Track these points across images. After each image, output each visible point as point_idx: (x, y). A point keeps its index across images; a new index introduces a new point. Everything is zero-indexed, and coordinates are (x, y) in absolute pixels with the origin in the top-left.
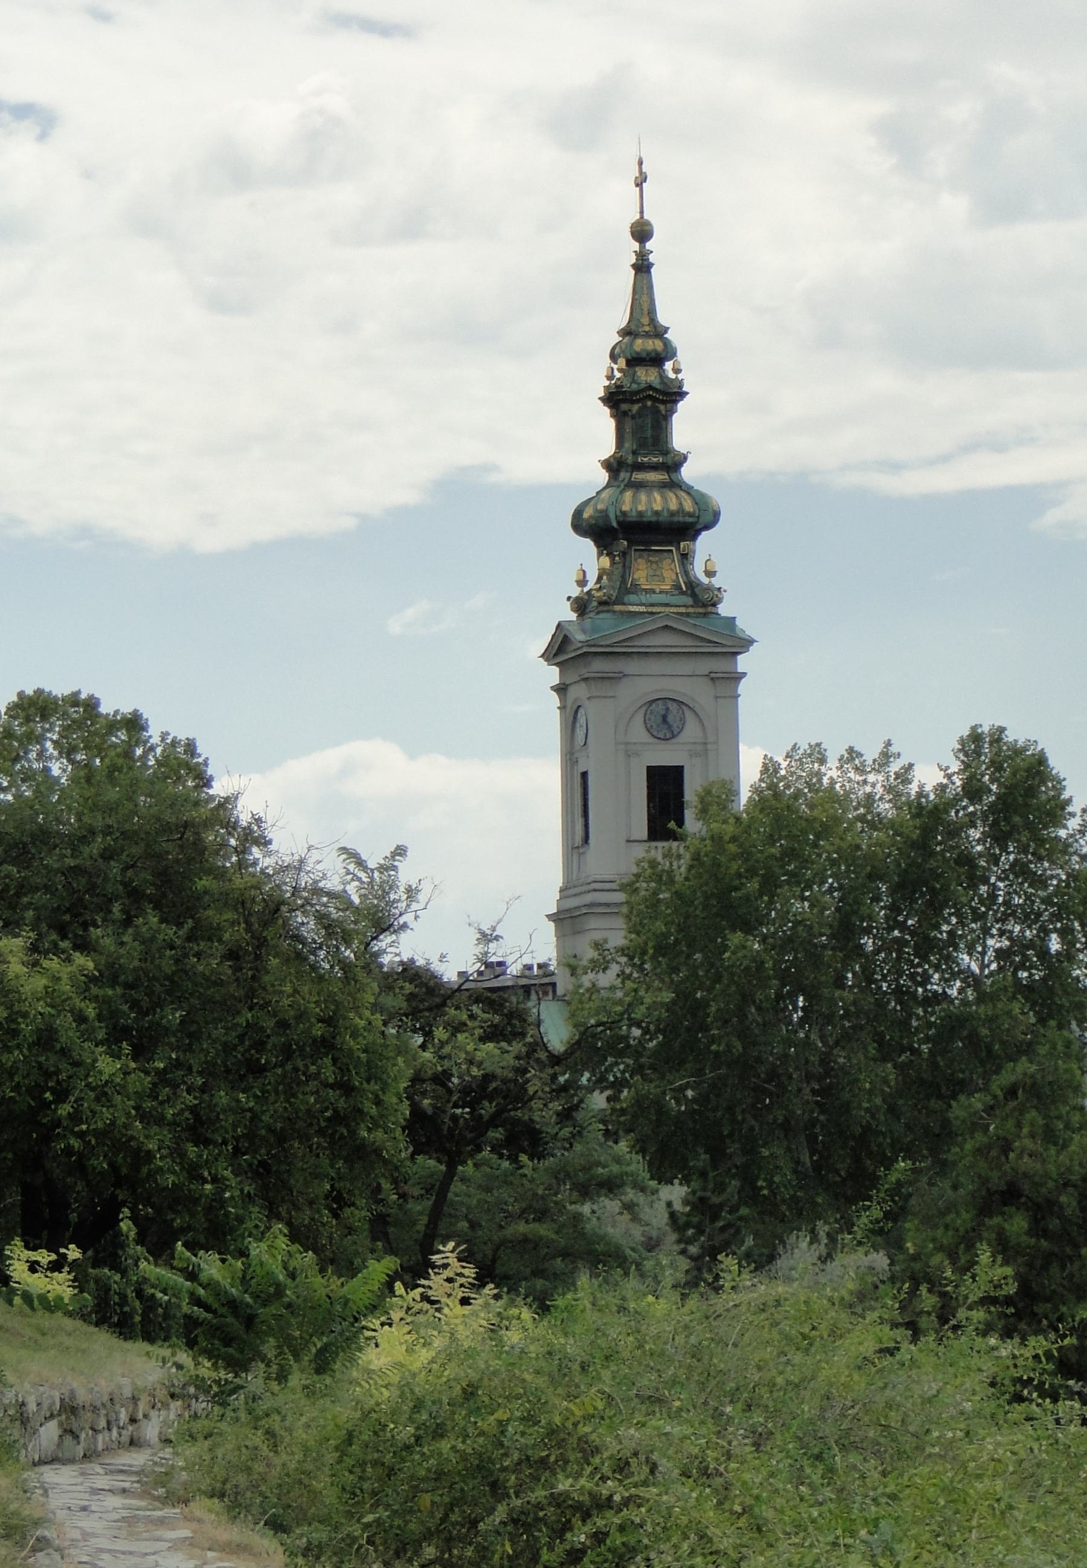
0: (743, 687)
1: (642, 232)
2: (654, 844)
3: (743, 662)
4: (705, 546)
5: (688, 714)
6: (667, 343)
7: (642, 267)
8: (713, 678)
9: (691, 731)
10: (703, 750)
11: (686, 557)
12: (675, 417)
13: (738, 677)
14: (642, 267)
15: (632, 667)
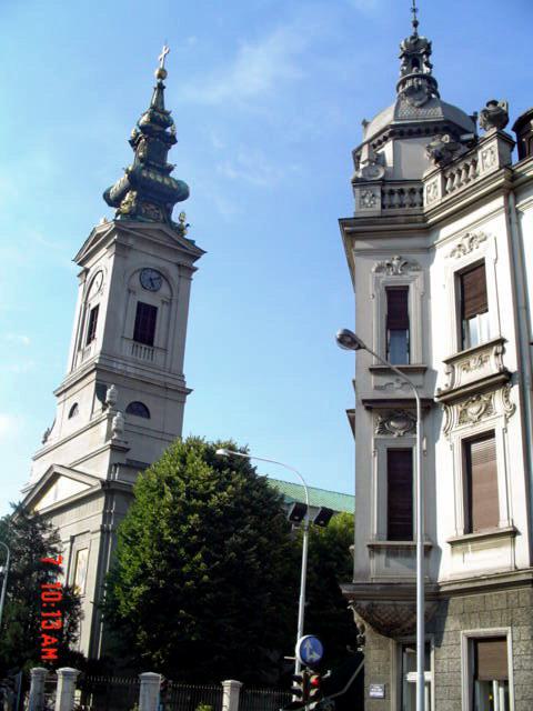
0: (194, 275)
1: (162, 75)
2: (136, 343)
3: (195, 264)
4: (178, 210)
5: (164, 283)
6: (169, 118)
7: (161, 88)
8: (179, 266)
9: (164, 290)
10: (169, 303)
11: (169, 211)
12: (169, 152)
13: (195, 269)
14: (161, 88)
15: (137, 246)
